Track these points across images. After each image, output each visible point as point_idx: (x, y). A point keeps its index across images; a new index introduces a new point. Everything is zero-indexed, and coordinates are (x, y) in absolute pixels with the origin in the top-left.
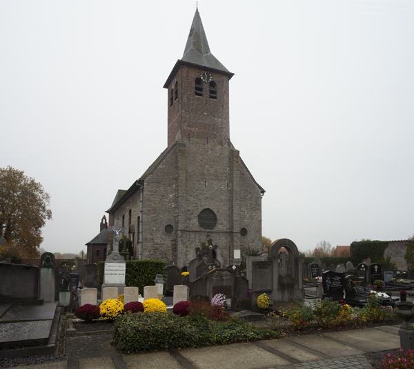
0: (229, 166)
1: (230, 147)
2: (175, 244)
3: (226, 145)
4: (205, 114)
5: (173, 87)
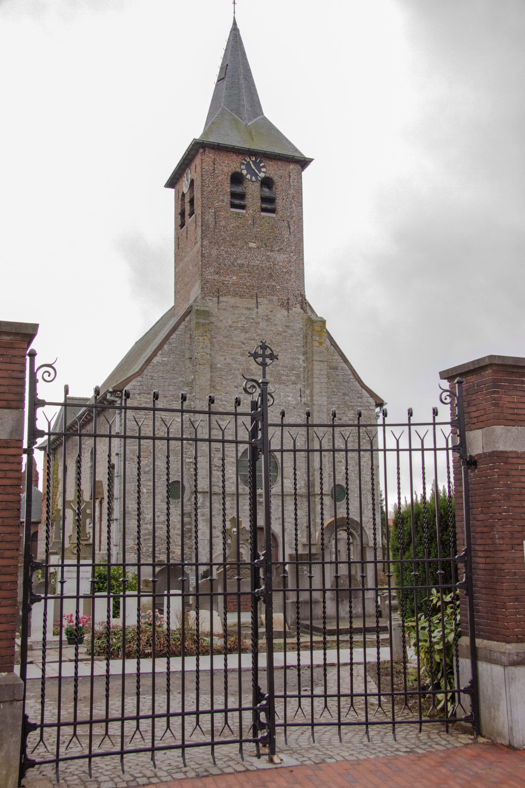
0: (305, 353)
1: (305, 312)
3: (297, 309)
4: (252, 245)
5: (185, 190)
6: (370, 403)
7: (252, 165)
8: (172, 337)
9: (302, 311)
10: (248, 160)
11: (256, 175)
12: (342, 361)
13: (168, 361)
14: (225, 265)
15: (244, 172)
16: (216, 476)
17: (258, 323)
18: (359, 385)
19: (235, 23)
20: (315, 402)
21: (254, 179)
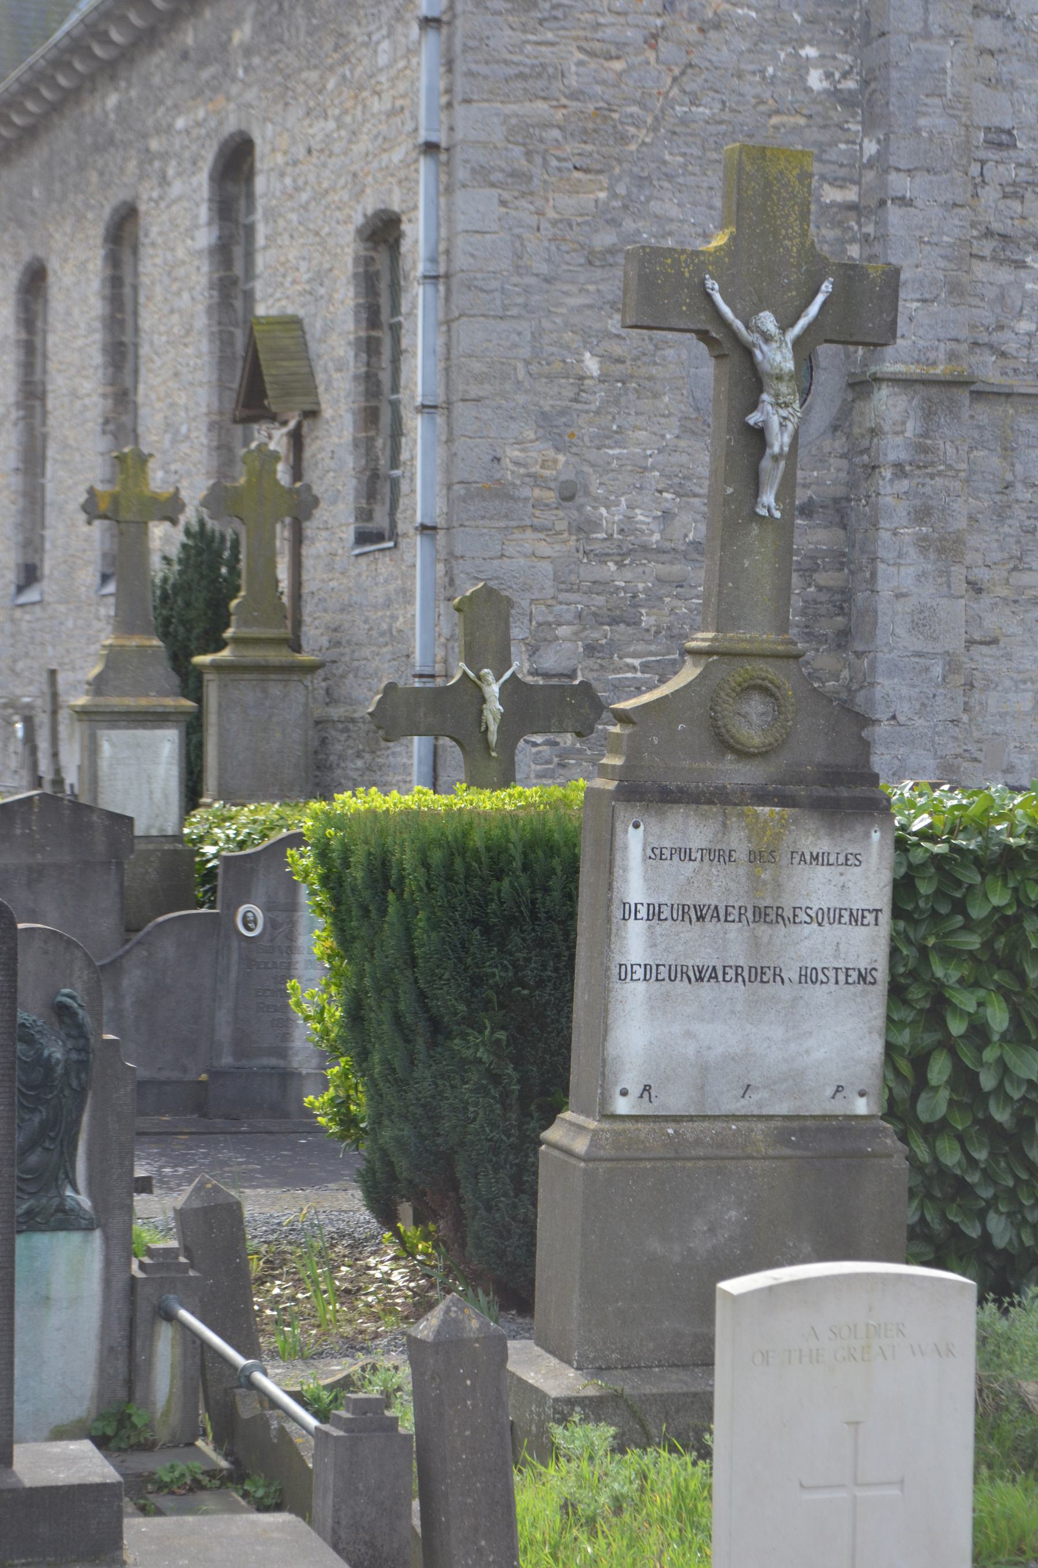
16: (991, 293)
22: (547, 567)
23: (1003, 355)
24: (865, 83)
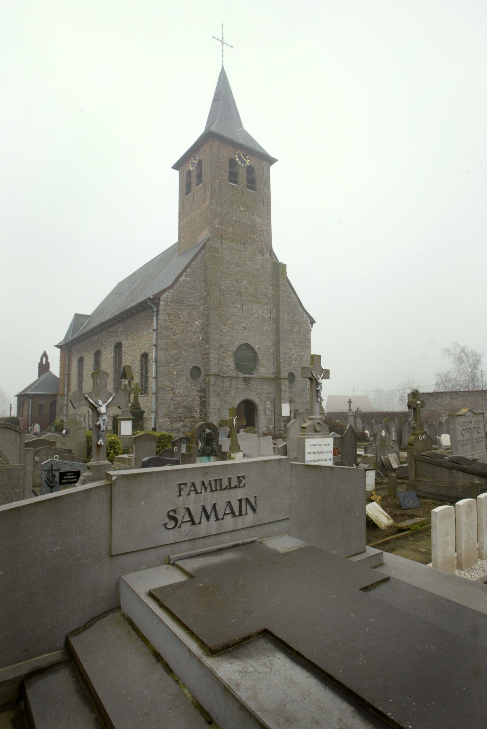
2: (204, 397)
3: (268, 256)
4: (241, 209)
6: (308, 321)
7: (242, 156)
8: (192, 264)
9: (270, 257)
10: (239, 152)
11: (245, 163)
12: (292, 293)
13: (190, 280)
14: (226, 219)
15: (237, 159)
17: (245, 261)
18: (302, 309)
19: (223, 68)
20: (281, 318)
21: (243, 165)
22: (170, 398)
23: (223, 371)
24: (207, 339)
